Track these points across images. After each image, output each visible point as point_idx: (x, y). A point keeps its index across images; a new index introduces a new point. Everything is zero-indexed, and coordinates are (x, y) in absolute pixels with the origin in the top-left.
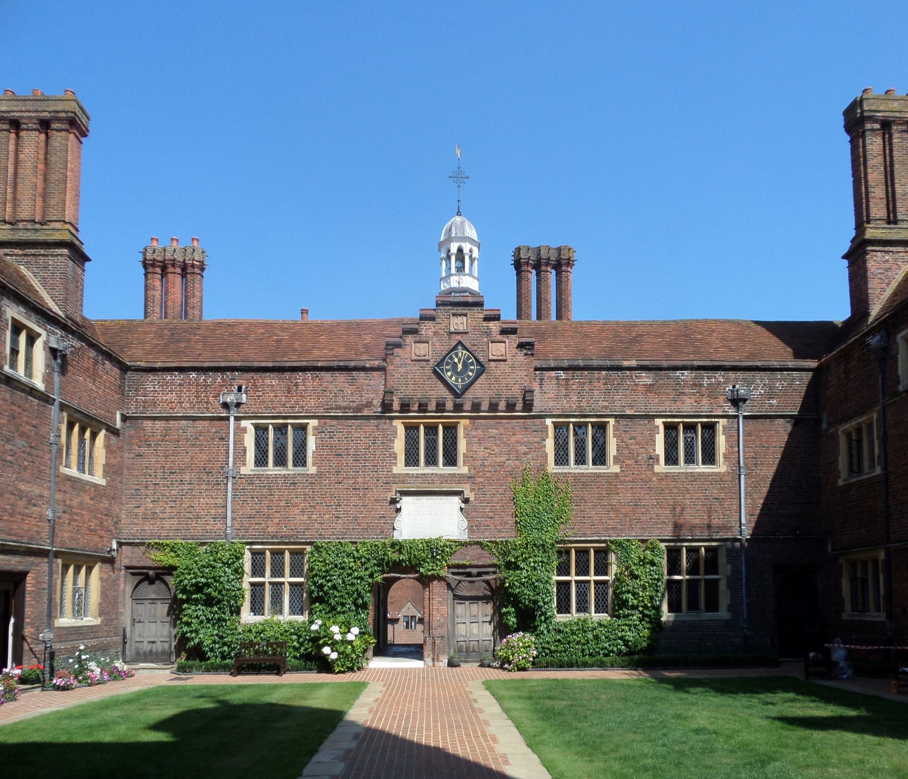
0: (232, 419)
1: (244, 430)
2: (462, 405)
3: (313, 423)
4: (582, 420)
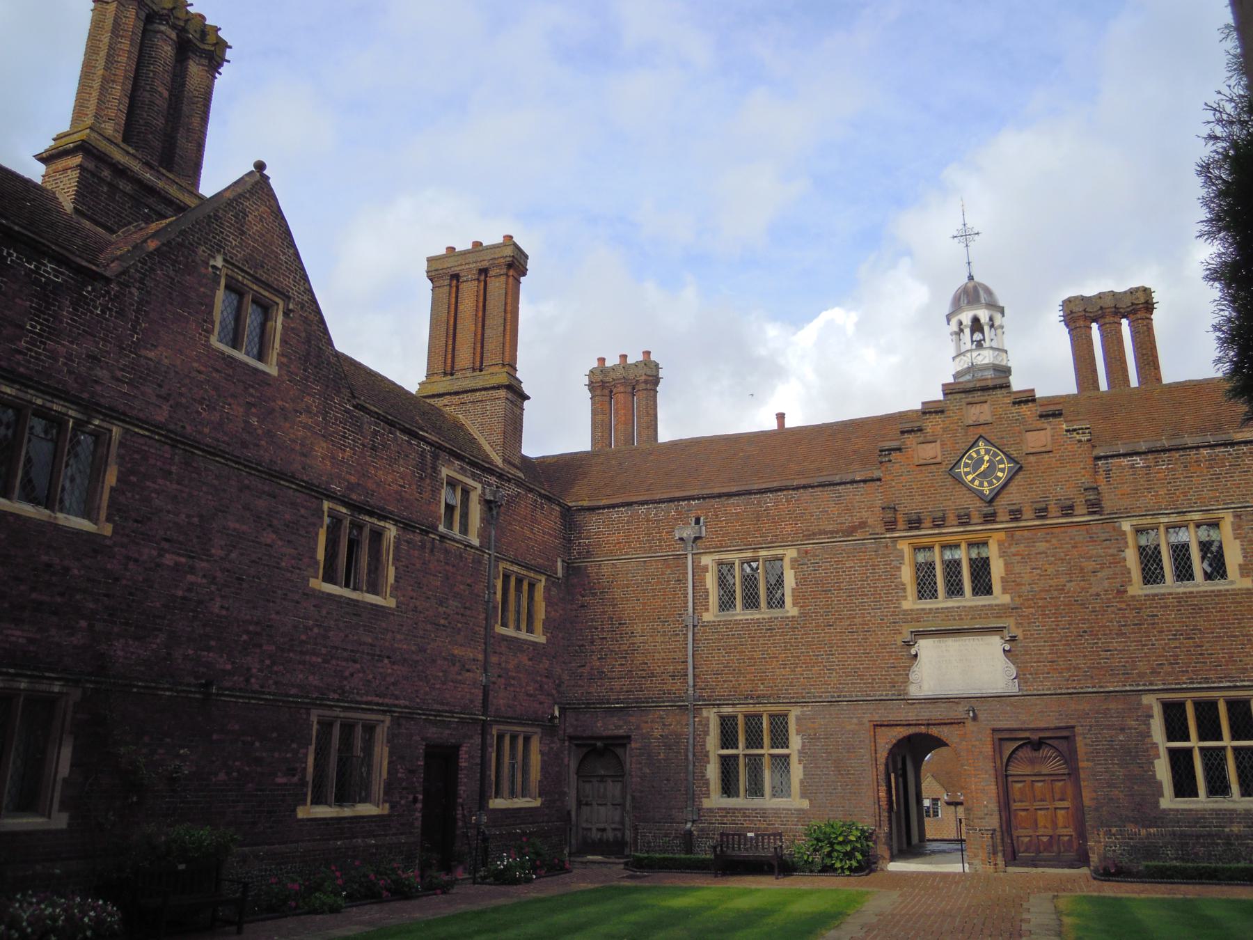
0: (690, 557)
1: (705, 569)
2: (994, 514)
3: (791, 553)
4: (1179, 519)
